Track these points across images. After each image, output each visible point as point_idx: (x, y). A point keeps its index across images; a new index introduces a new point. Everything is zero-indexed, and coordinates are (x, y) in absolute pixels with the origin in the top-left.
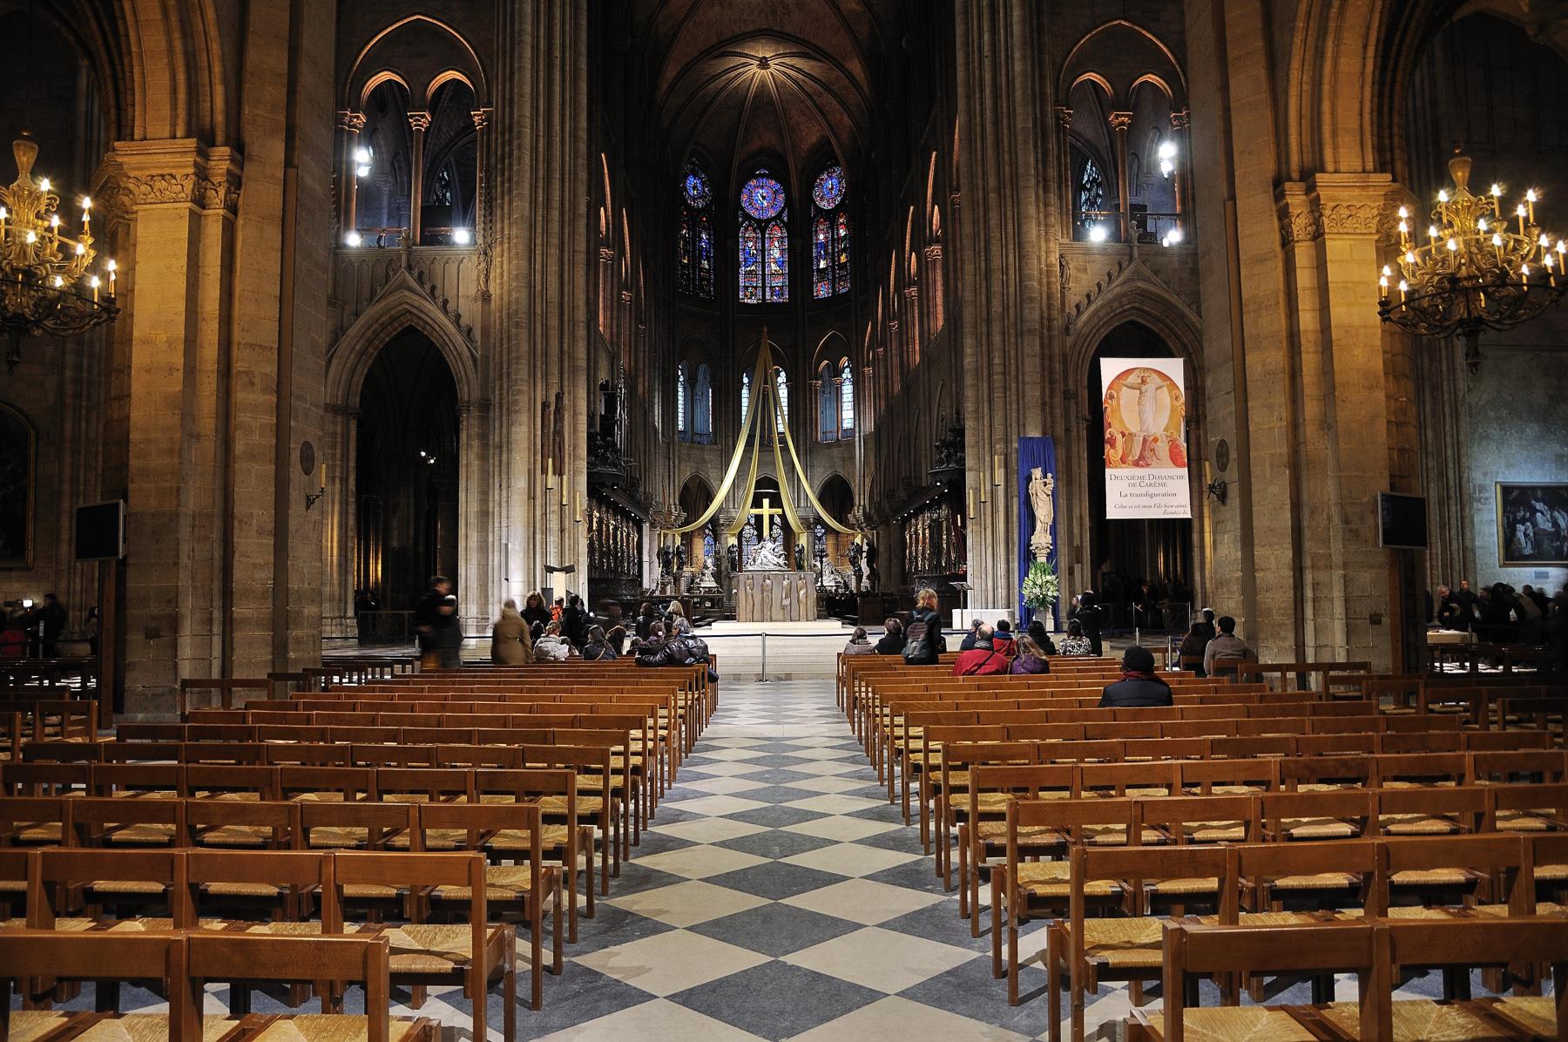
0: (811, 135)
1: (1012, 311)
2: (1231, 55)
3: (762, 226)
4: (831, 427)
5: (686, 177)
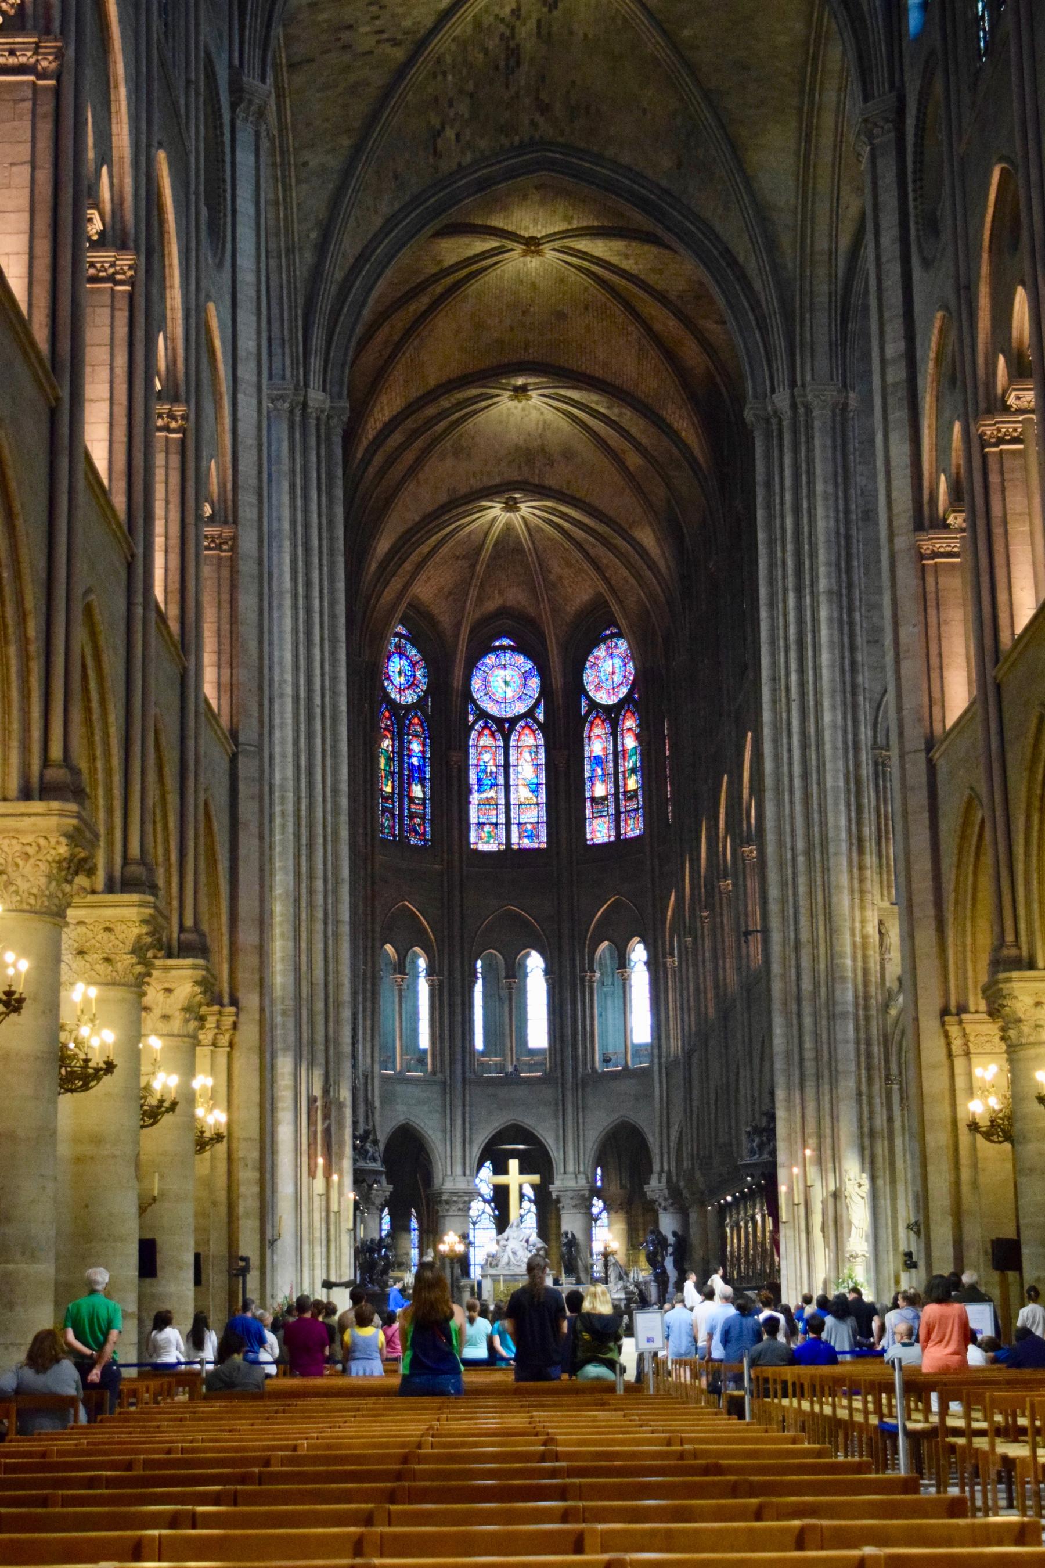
0: (580, 591)
1: (823, 990)
2: (917, 913)
3: (504, 727)
4: (614, 1045)
5: (389, 658)
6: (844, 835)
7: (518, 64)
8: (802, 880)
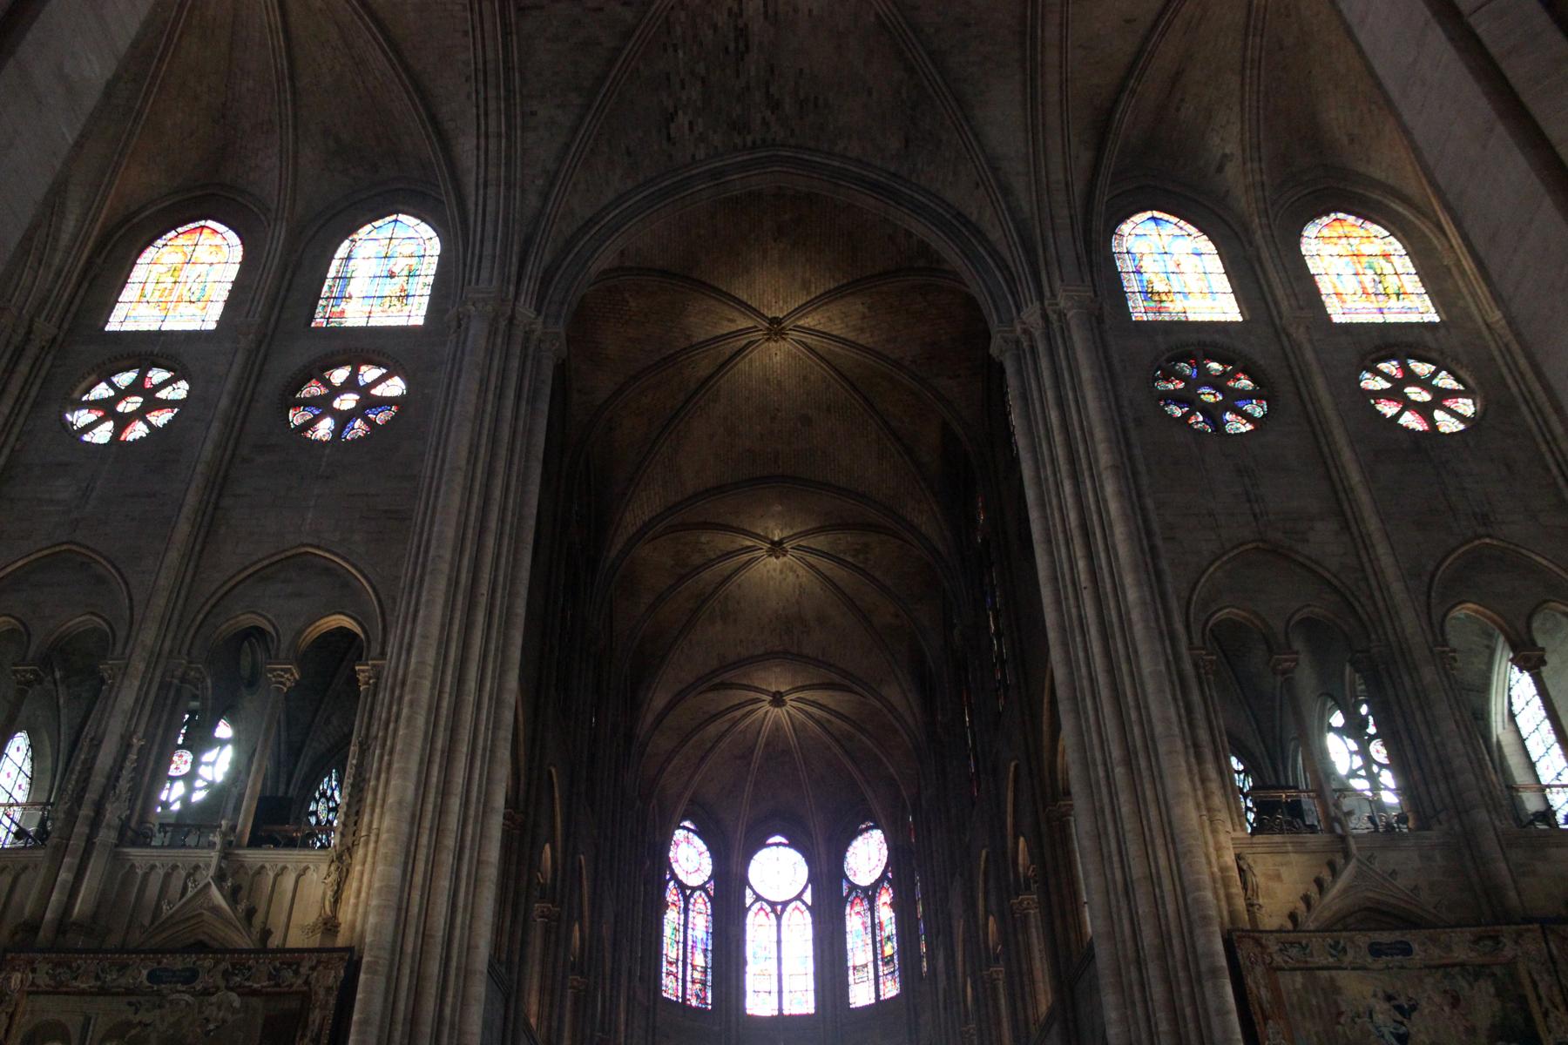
1: (1176, 942)
3: (778, 909)
6: (1176, 730)
7: (747, 47)
8: (1124, 798)
